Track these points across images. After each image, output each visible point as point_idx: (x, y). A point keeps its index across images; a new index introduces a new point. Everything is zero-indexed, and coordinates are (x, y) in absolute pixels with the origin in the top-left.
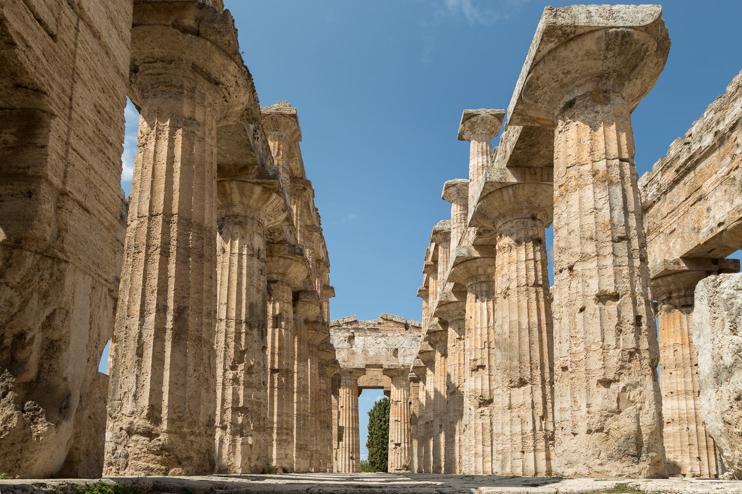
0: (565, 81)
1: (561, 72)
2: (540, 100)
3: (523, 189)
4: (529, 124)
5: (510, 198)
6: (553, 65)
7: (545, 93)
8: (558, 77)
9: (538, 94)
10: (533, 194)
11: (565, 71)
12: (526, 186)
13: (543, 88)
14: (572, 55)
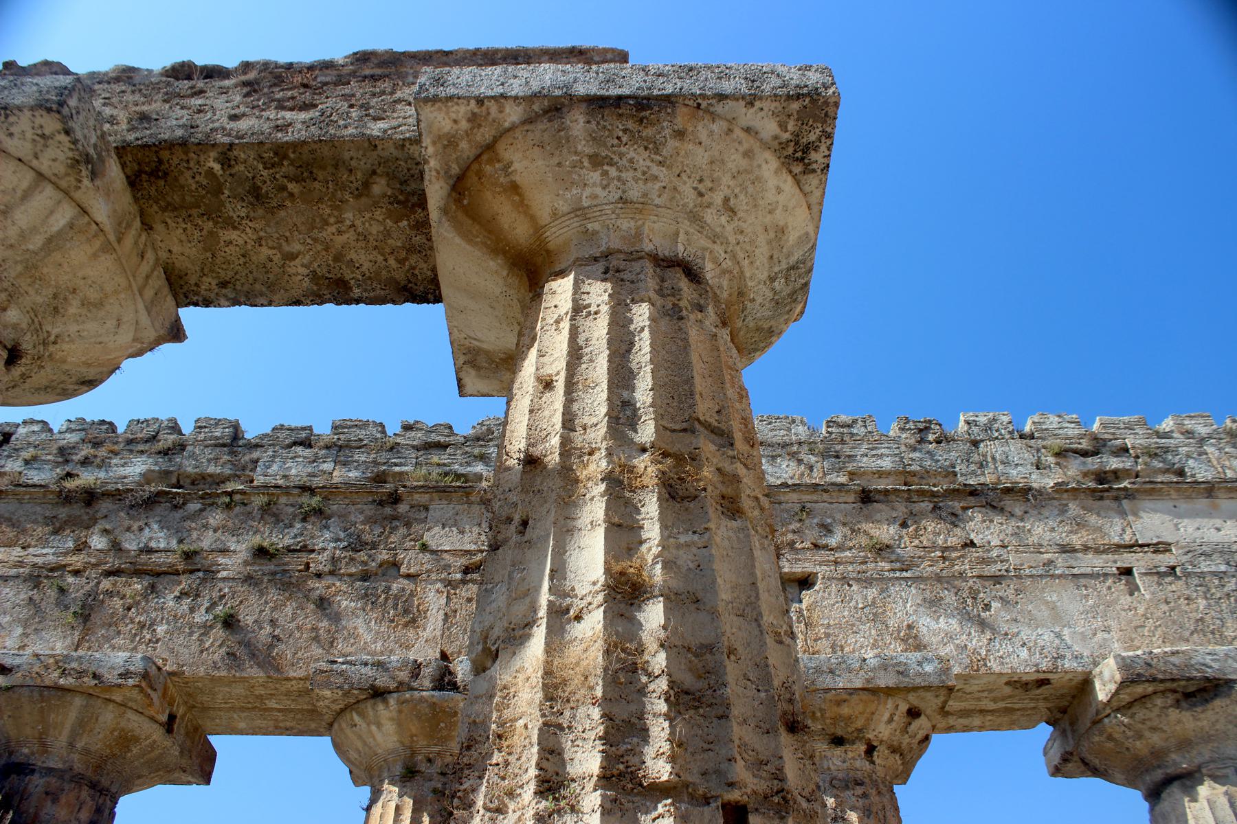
0: (710, 216)
1: (727, 192)
2: (613, 172)
3: (95, 256)
5: (34, 230)
6: (735, 160)
7: (649, 178)
10: (93, 295)
11: (732, 202)
12: (106, 261)
14: (770, 196)
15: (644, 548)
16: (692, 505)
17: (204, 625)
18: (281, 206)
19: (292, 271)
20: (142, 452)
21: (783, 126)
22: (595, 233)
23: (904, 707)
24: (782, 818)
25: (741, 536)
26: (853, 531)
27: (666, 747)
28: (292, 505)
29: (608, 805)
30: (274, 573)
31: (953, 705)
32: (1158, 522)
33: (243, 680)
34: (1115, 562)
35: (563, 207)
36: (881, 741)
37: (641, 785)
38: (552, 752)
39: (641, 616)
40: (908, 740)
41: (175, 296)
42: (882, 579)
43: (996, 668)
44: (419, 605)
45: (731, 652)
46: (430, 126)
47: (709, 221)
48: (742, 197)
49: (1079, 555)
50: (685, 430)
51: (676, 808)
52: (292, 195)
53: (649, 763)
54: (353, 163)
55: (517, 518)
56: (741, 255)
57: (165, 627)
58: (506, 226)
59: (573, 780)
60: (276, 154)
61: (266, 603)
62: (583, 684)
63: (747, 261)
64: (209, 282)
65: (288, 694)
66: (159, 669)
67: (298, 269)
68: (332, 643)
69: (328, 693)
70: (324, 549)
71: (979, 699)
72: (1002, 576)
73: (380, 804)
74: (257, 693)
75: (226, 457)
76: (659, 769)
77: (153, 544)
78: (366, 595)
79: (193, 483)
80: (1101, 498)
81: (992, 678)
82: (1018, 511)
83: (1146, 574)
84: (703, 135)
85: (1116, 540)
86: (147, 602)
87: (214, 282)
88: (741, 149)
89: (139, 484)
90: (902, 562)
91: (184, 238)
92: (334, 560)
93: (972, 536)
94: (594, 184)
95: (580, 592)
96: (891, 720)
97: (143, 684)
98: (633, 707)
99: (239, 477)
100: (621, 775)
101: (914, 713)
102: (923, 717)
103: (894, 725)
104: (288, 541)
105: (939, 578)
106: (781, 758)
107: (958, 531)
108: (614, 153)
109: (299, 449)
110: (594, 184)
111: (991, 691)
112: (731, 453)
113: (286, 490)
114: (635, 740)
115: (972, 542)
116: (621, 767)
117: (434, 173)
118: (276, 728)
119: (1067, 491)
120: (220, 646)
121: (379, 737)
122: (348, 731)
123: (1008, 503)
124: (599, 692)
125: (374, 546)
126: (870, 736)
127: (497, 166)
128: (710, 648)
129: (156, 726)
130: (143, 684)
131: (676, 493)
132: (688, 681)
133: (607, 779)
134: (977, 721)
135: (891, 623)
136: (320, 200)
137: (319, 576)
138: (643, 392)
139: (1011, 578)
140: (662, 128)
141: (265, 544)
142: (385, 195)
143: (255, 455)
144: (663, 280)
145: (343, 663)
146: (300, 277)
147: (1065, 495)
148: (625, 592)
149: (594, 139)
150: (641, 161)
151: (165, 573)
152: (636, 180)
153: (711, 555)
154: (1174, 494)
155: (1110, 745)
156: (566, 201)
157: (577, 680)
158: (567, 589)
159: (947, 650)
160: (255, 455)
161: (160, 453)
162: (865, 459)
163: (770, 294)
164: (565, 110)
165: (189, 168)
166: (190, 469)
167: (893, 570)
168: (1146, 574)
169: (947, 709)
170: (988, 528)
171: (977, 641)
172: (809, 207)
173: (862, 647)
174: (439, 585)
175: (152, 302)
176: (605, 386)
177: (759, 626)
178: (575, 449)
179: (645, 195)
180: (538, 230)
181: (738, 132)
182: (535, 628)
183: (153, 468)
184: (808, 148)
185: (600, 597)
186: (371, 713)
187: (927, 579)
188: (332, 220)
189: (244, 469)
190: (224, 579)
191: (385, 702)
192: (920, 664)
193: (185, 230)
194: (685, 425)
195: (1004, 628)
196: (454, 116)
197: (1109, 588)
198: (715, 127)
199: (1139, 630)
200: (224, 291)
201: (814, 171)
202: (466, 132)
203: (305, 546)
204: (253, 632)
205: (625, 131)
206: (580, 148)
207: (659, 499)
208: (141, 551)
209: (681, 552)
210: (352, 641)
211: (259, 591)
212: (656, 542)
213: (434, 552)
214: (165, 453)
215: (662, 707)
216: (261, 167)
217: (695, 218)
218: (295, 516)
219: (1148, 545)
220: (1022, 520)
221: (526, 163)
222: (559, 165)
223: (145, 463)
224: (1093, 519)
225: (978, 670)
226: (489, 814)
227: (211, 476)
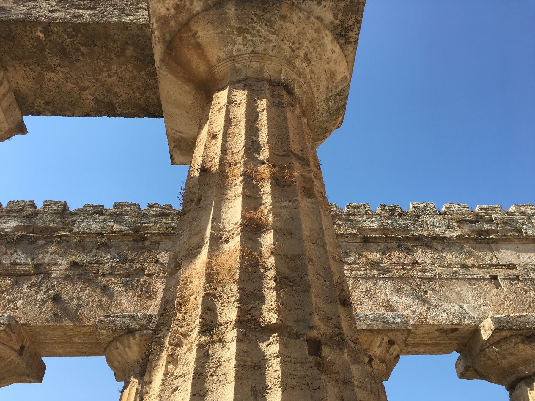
0: (297, 63)
2: (249, 37)
4: (156, 33)
6: (311, 33)
8: (299, 48)
9: (259, 28)
13: (273, 33)
14: (328, 54)
15: (263, 207)
16: (288, 189)
17: (42, 300)
18: (78, 60)
19: (84, 97)
20: (15, 217)
21: (335, 16)
22: (240, 69)
23: (386, 339)
24: (341, 349)
25: (314, 206)
26: (360, 255)
27: (274, 305)
28: (92, 242)
29: (241, 337)
30: (81, 274)
31: (410, 340)
32: (509, 255)
33: (61, 327)
34: (488, 273)
35: (223, 55)
36: (376, 356)
37: (260, 326)
38: (209, 310)
39: (261, 240)
40: (389, 357)
41: (21, 109)
42: (374, 278)
43: (431, 322)
44: (153, 289)
45: (310, 260)
46: (154, 11)
47: (297, 65)
48: (314, 53)
49: (470, 269)
50: (285, 155)
51: (280, 338)
52: (83, 54)
53: (265, 314)
54: (116, 37)
55: (196, 199)
56: (313, 85)
57: (22, 301)
58: (194, 67)
59: (221, 325)
60: (74, 29)
61: (76, 289)
62: (228, 273)
63: (315, 89)
64: (39, 102)
65: (85, 334)
66: (17, 322)
67: (87, 96)
68: (108, 308)
69: (104, 332)
70: (107, 263)
71: (423, 338)
72: (432, 278)
73: (128, 388)
74: (68, 334)
75: (59, 219)
76: (271, 317)
77: (18, 261)
78: (127, 284)
79: (41, 232)
80: (481, 243)
81: (429, 327)
82: (439, 248)
83: (504, 279)
84: (295, 19)
85: (489, 262)
86: (13, 289)
87: (42, 102)
88: (314, 28)
89: (12, 231)
90: (384, 271)
91: (25, 76)
92: (112, 268)
93: (417, 259)
94: (239, 44)
95: (228, 228)
96: (380, 346)
97: (8, 330)
98: (256, 285)
99: (65, 229)
100: (248, 320)
101: (391, 343)
102: (396, 345)
103: (382, 348)
104: (89, 259)
105: (401, 278)
106: (339, 316)
107: (410, 257)
108: (250, 27)
109: (97, 216)
110: (239, 44)
111: (429, 334)
112: (308, 168)
113: (89, 235)
114: (257, 302)
115: (417, 261)
116: (249, 316)
117: (157, 39)
118: (78, 352)
119: (463, 239)
120: (50, 310)
121: (130, 354)
122: (114, 352)
123: (434, 244)
124: (237, 276)
125: (133, 261)
126: (371, 354)
127: (190, 34)
128: (299, 257)
129: (13, 352)
130: (8, 330)
131: (279, 183)
132: (287, 272)
133: (240, 323)
134: (422, 349)
135: (379, 299)
136: (99, 58)
137: (104, 275)
138: (263, 137)
139: (437, 279)
140: (274, 14)
141: (77, 260)
142: (132, 56)
143: (74, 218)
144: (274, 91)
145: (113, 317)
146: (89, 101)
147: (462, 241)
148: (252, 229)
149: (240, 19)
150: (263, 31)
151: (24, 275)
152: (261, 41)
153: (299, 212)
154: (517, 242)
155: (489, 362)
156: (225, 52)
157: (225, 272)
158: (221, 227)
159: (407, 312)
160: (74, 218)
161: (24, 217)
162: (365, 223)
163: (326, 108)
164: (225, 4)
165: (26, 36)
166: (39, 225)
167: (379, 274)
168: (504, 279)
169: (407, 342)
170: (425, 255)
171: (421, 309)
172: (347, 62)
173: (365, 310)
174: (163, 279)
175: (7, 109)
176: (243, 134)
177: (325, 249)
178: (227, 163)
179: (265, 50)
180: (210, 68)
181: (312, 18)
182: (203, 248)
183: (20, 224)
184: (348, 29)
185: (239, 230)
186: (126, 342)
187: (396, 278)
188: (105, 69)
189: (68, 225)
190: (54, 278)
191: (134, 336)
192: (394, 318)
193: (25, 71)
194: (284, 153)
195: (435, 303)
196: (167, 6)
197: (486, 285)
198: (301, 15)
199: (502, 305)
200: (48, 107)
201: (350, 43)
202: (173, 15)
203: (98, 261)
204: (68, 303)
205: (255, 15)
206: (232, 23)
207: (271, 184)
208: (11, 264)
209: (283, 210)
210: (119, 306)
211: (72, 283)
212: (269, 204)
213: (162, 264)
214: (27, 217)
215: (273, 284)
216: (66, 37)
217: (290, 63)
218: (93, 247)
219: (505, 265)
220: (441, 252)
221: (204, 32)
222: (221, 33)
223: (16, 222)
224: (477, 252)
225: (422, 323)
226: (171, 347)
227: (51, 228)
